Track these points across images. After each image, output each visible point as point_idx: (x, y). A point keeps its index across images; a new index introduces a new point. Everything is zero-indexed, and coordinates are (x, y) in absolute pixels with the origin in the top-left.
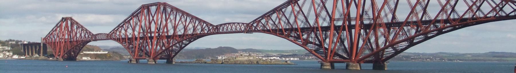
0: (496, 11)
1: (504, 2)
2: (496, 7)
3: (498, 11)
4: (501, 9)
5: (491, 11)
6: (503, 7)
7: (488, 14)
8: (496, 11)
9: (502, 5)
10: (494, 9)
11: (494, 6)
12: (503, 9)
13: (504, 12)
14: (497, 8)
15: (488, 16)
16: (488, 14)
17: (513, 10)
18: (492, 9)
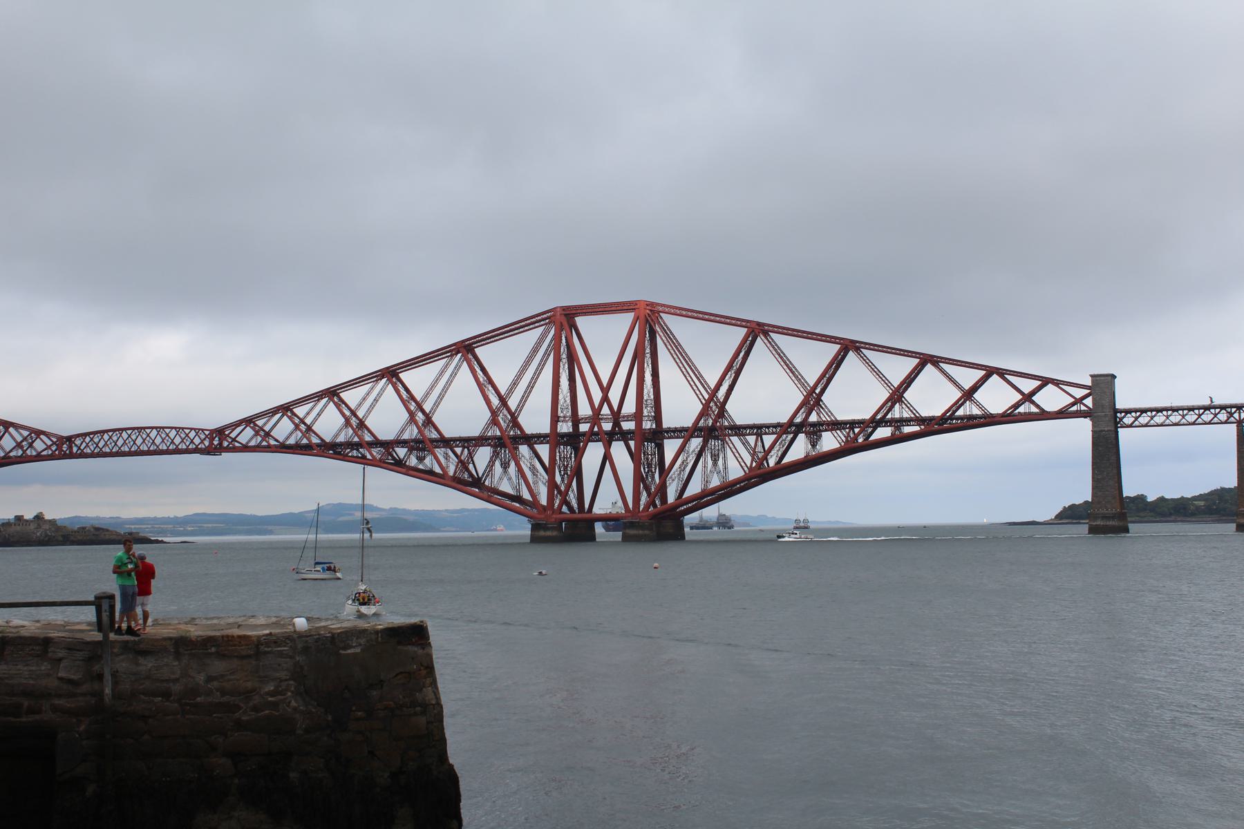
0: (22, 447)
1: (33, 435)
2: (22, 441)
3: (25, 448)
4: (31, 445)
5: (14, 448)
6: (33, 442)
7: (11, 451)
8: (22, 447)
9: (32, 439)
10: (19, 445)
11: (19, 439)
12: (34, 444)
13: (35, 450)
14: (24, 443)
15: (42, 454)
16: (11, 451)
17: (46, 447)
18: (15, 444)
